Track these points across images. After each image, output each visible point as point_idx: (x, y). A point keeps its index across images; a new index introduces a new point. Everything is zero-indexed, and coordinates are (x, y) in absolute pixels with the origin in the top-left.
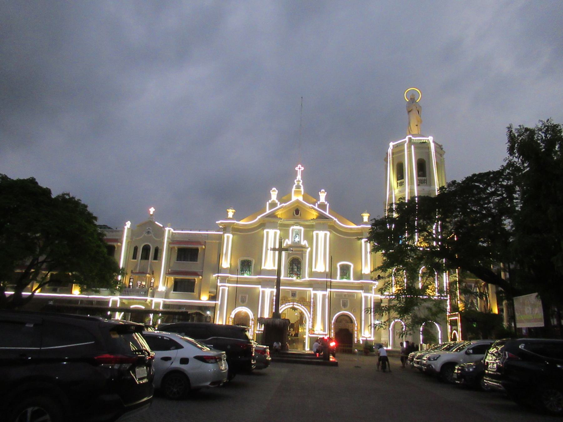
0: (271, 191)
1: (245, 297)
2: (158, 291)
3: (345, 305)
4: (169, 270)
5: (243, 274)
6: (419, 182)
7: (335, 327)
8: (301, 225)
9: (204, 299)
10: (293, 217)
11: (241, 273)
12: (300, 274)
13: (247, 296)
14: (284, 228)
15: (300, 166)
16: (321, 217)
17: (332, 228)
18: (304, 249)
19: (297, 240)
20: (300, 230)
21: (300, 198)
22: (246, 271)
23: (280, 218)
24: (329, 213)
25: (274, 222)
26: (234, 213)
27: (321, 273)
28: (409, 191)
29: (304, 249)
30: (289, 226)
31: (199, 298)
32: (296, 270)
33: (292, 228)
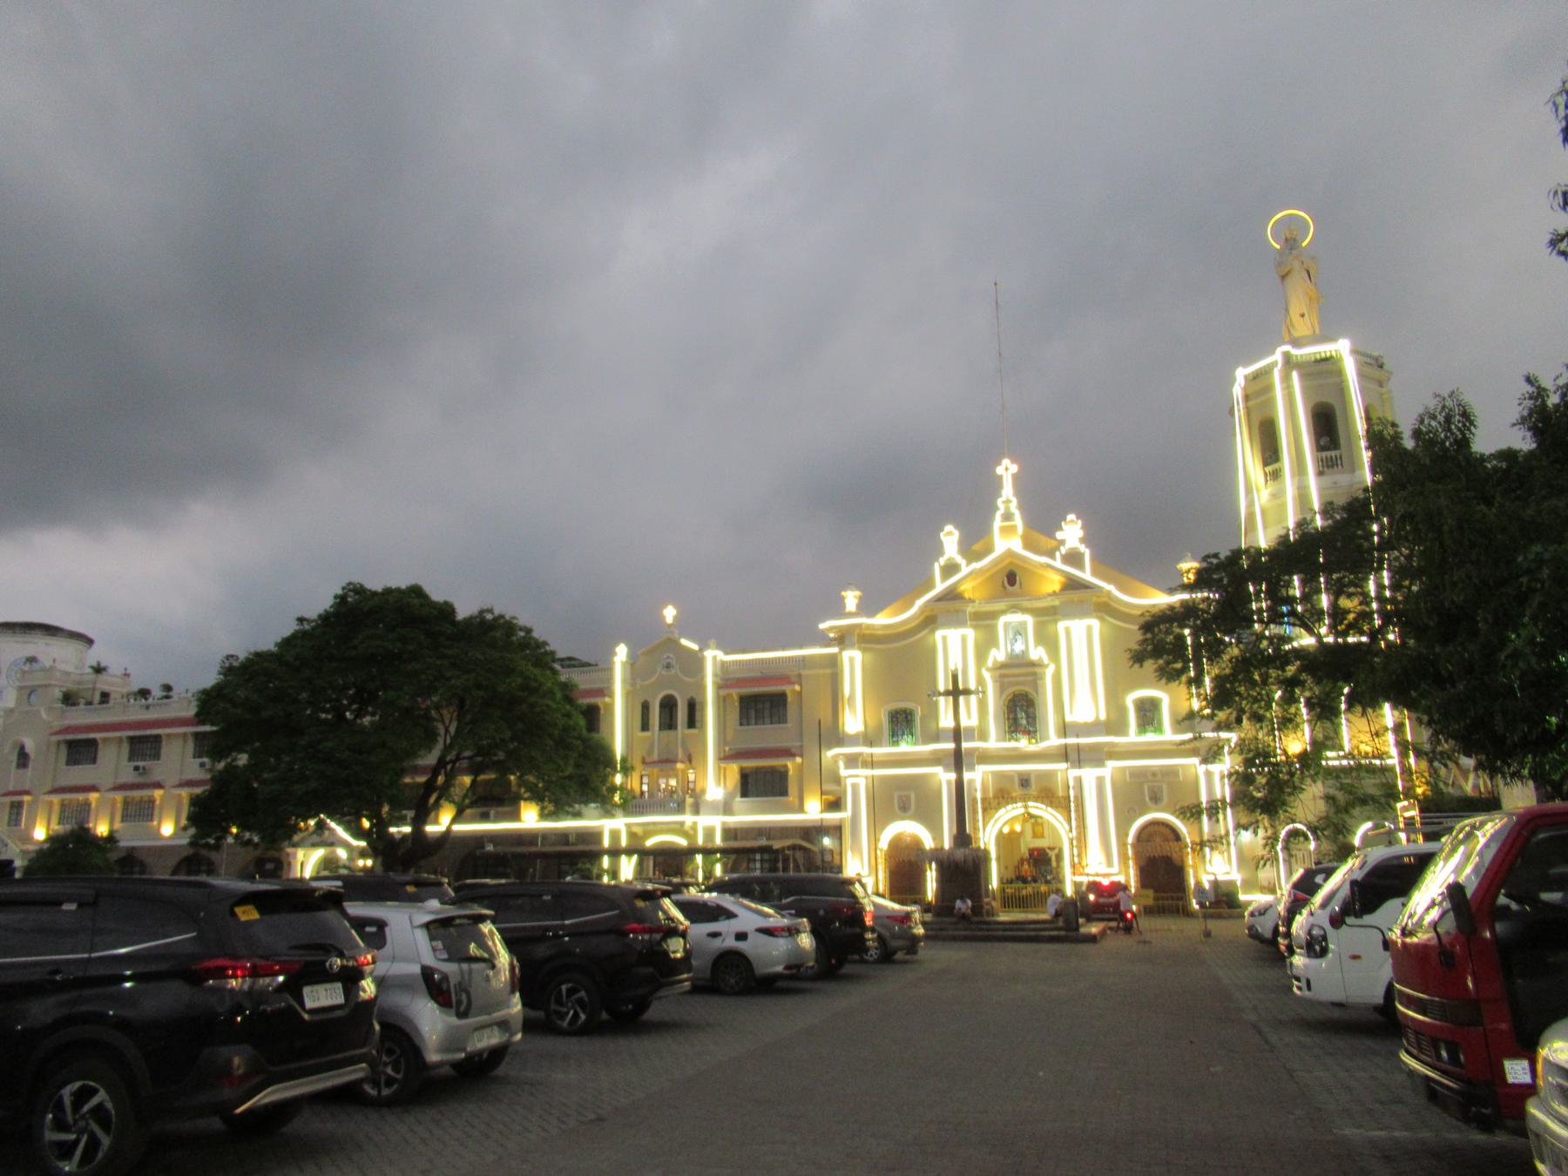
0: (942, 534)
1: (908, 798)
2: (707, 801)
3: (1156, 799)
4: (724, 751)
5: (896, 743)
6: (1320, 463)
7: (1137, 855)
8: (1025, 610)
9: (813, 811)
10: (1005, 595)
11: (893, 742)
12: (1036, 732)
13: (913, 796)
14: (985, 621)
15: (1006, 462)
16: (1073, 585)
17: (1106, 609)
18: (1037, 670)
19: (1019, 647)
20: (1023, 624)
21: (1014, 543)
22: (903, 734)
23: (970, 599)
24: (1095, 573)
25: (957, 611)
26: (860, 598)
27: (1086, 725)
28: (1296, 492)
29: (1037, 670)
30: (993, 615)
31: (801, 809)
32: (1024, 722)
33: (1003, 620)
